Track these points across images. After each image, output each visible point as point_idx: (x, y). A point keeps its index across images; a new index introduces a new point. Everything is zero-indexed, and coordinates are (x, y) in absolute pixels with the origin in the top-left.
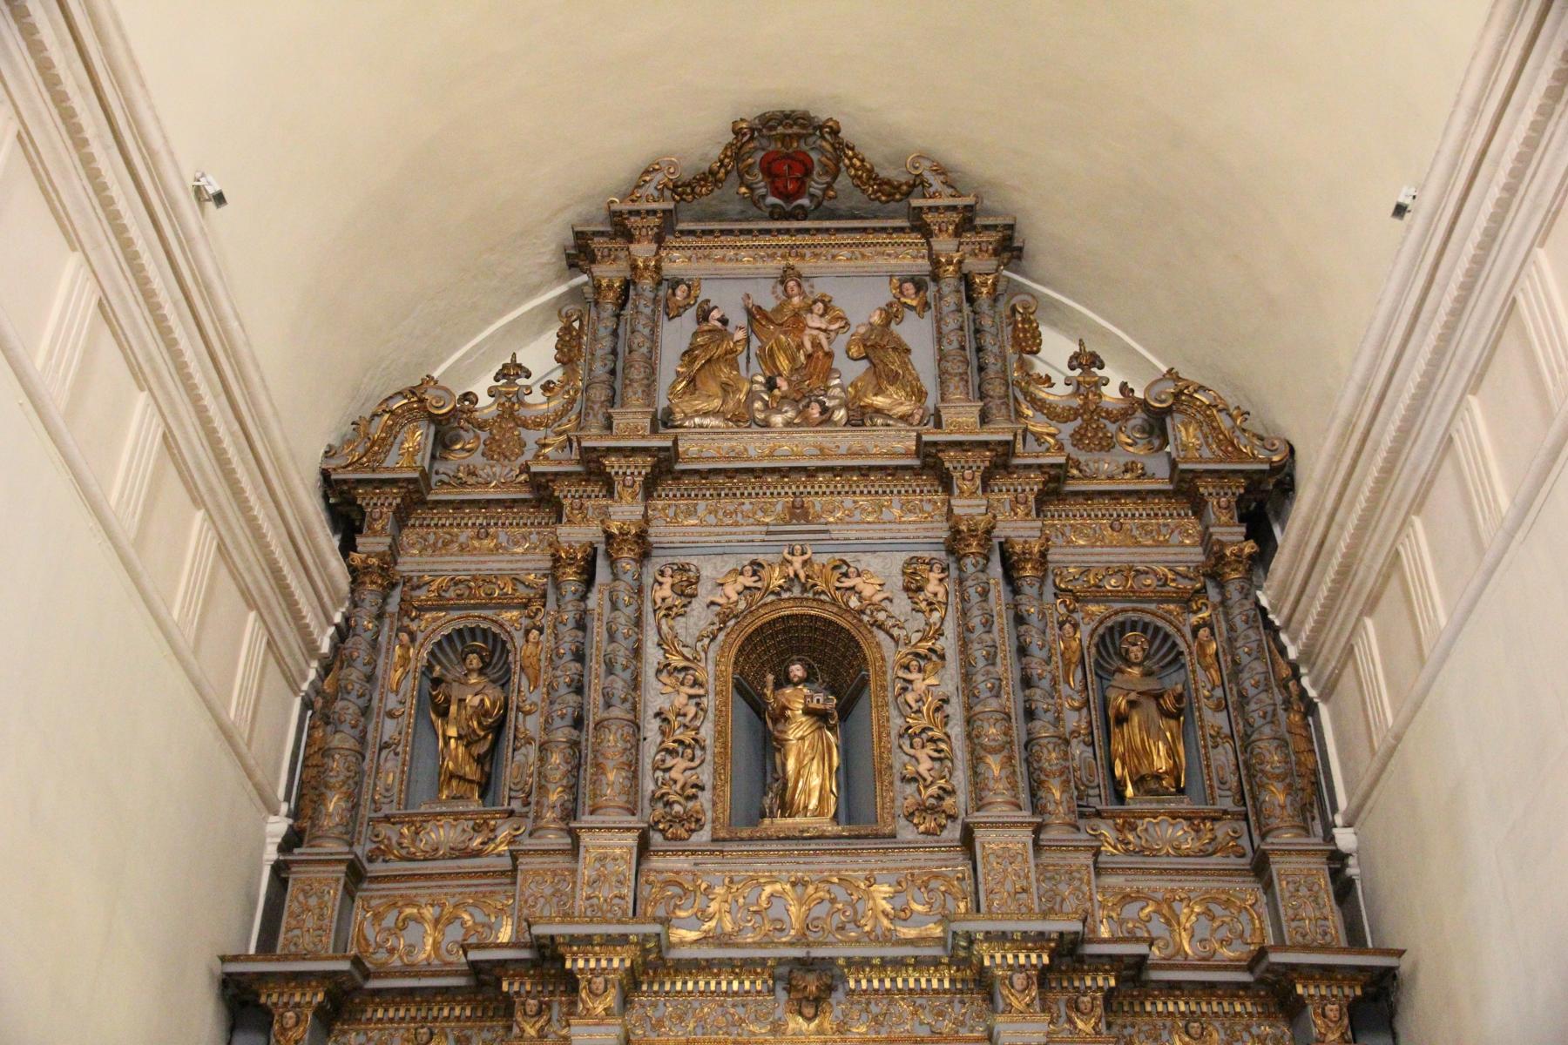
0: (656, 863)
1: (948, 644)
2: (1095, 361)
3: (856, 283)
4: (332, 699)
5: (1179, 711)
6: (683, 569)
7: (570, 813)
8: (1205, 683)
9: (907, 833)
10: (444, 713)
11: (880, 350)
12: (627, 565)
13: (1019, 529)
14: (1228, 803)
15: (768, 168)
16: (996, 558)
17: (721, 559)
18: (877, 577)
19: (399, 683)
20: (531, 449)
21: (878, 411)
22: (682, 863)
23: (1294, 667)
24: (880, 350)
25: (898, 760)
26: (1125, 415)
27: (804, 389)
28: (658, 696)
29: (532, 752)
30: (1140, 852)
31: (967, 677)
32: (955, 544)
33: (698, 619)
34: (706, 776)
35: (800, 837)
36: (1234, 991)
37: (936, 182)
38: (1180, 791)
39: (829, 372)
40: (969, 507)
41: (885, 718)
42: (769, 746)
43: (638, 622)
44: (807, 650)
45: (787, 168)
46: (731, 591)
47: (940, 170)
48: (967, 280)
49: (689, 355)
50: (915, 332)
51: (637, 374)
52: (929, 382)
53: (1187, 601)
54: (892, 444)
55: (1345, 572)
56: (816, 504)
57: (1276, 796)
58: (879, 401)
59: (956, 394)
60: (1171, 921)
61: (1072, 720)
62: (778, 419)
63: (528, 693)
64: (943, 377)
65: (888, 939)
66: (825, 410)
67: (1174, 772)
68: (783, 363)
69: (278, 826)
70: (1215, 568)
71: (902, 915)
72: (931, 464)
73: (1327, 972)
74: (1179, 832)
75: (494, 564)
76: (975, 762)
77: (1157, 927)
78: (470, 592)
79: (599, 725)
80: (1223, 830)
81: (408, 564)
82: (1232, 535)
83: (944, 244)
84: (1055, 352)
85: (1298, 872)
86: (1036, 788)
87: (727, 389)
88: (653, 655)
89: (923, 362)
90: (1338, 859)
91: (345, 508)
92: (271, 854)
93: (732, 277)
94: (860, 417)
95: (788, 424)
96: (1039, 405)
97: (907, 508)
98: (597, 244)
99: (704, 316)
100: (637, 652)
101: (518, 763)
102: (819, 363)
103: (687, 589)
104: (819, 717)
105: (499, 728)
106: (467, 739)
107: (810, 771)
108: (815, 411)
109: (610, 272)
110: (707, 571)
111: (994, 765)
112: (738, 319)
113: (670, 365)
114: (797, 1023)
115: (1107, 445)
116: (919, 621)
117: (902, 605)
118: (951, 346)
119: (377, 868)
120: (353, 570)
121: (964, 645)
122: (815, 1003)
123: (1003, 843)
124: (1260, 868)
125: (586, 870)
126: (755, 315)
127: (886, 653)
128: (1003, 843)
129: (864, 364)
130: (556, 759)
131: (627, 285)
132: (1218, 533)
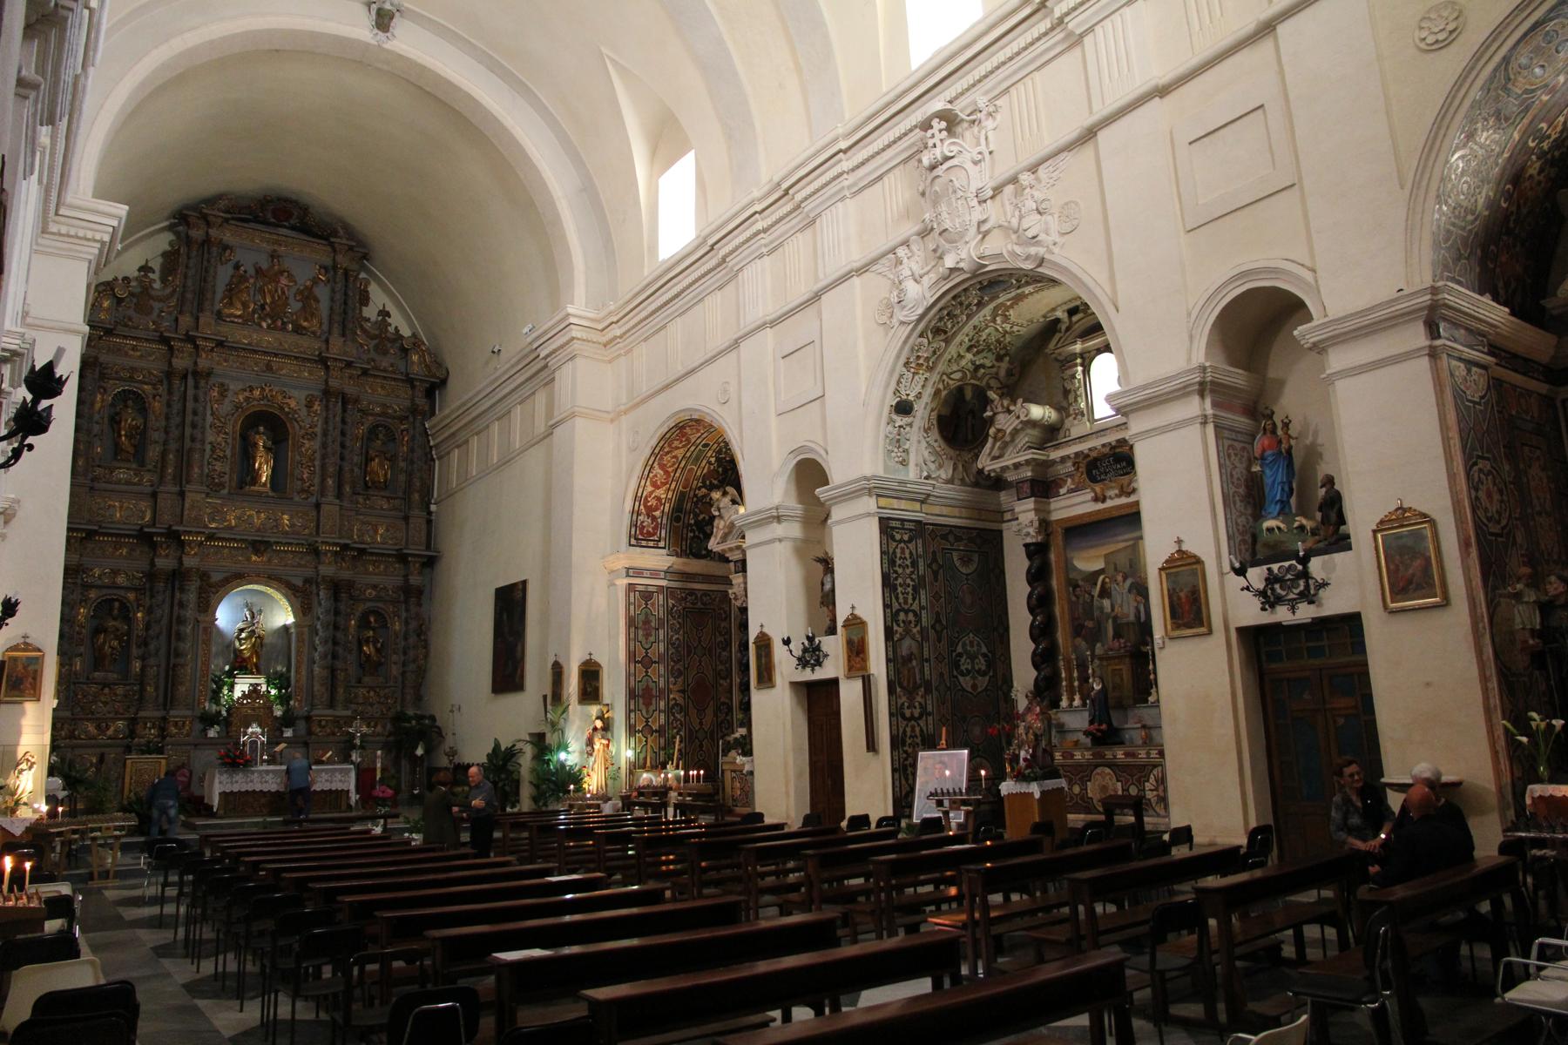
1: (318, 430)
2: (388, 314)
3: (304, 263)
5: (393, 459)
6: (222, 385)
9: (297, 499)
13: (351, 389)
14: (400, 494)
17: (235, 387)
18: (295, 401)
24: (307, 296)
25: (297, 472)
26: (393, 341)
27: (275, 315)
29: (158, 448)
31: (324, 446)
32: (327, 393)
33: (226, 407)
34: (227, 470)
35: (260, 494)
37: (341, 232)
39: (286, 304)
42: (247, 454)
45: (280, 212)
47: (347, 227)
48: (346, 273)
50: (322, 293)
53: (402, 419)
54: (309, 345)
55: (453, 434)
57: (416, 496)
60: (376, 532)
66: (284, 323)
70: (414, 410)
71: (292, 525)
72: (323, 361)
76: (323, 480)
79: (190, 450)
80: (397, 502)
81: (103, 358)
82: (421, 401)
85: (417, 520)
87: (245, 305)
88: (209, 419)
90: (430, 513)
93: (250, 248)
94: (298, 330)
96: (364, 330)
99: (237, 267)
101: (153, 452)
103: (223, 394)
109: (197, 234)
112: (251, 271)
114: (254, 558)
115: (385, 353)
117: (304, 410)
119: (97, 485)
122: (257, 552)
124: (406, 519)
126: (259, 271)
128: (330, 508)
129: (300, 305)
132: (417, 401)
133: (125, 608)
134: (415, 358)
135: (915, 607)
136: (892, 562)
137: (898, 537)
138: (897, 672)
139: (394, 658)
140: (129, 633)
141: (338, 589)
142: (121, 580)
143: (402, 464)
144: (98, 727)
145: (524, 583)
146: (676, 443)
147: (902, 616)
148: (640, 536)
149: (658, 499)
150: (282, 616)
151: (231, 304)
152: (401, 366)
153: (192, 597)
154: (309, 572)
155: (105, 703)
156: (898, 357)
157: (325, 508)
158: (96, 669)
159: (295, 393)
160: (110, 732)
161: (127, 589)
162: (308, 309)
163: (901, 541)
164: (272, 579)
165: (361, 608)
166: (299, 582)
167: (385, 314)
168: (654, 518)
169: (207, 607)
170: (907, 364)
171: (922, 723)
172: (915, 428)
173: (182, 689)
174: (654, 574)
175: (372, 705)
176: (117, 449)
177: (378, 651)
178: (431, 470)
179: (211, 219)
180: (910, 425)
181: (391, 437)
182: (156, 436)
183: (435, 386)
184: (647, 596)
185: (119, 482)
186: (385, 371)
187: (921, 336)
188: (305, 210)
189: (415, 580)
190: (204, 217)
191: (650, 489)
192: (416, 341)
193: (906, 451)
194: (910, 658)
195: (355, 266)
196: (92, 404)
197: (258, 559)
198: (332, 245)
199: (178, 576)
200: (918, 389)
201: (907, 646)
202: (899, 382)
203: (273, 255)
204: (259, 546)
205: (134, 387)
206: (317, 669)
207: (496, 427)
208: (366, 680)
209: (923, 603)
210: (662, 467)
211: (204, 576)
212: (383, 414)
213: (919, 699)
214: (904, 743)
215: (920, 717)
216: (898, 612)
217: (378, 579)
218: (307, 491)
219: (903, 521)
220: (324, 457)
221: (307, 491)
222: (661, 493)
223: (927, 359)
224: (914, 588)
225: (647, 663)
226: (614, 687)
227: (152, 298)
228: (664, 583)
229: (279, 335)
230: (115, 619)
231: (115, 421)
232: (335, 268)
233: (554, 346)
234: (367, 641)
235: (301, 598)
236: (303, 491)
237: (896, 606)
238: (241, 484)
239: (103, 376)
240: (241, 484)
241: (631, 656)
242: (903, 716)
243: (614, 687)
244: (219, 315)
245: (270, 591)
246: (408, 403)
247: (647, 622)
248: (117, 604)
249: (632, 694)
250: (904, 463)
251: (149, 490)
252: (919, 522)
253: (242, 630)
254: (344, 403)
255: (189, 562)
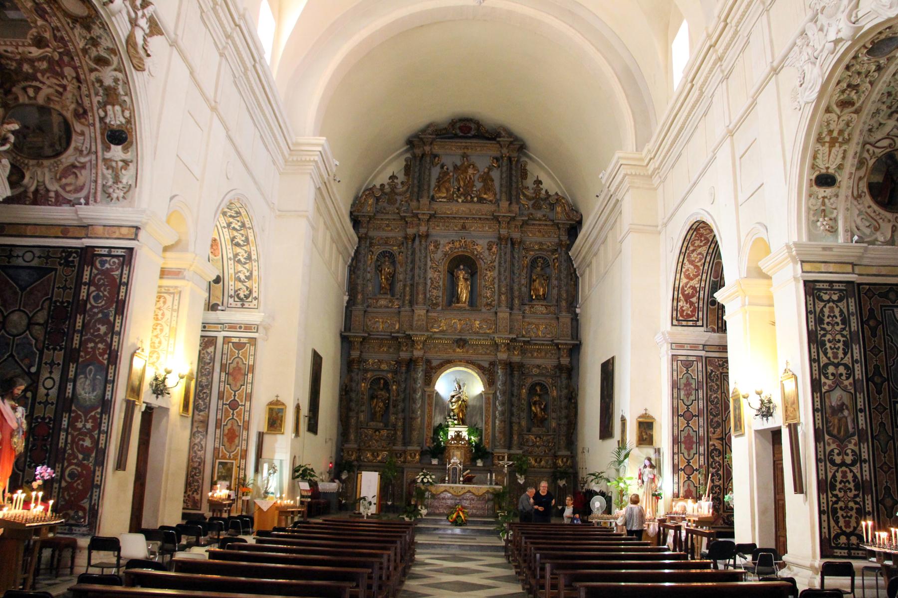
0: (430, 314)
1: (496, 264)
2: (541, 183)
3: (482, 158)
4: (354, 269)
6: (436, 241)
7: (411, 303)
8: (554, 273)
9: (484, 310)
10: (381, 271)
11: (486, 178)
12: (423, 242)
13: (516, 235)
14: (554, 303)
15: (461, 128)
16: (509, 242)
17: (445, 241)
18: (481, 247)
19: (370, 260)
20: (399, 202)
21: (485, 199)
22: (435, 314)
23: (575, 270)
24: (486, 178)
27: (466, 193)
28: (430, 274)
30: (534, 313)
31: (500, 273)
33: (439, 255)
35: (460, 309)
36: (547, 345)
37: (503, 134)
38: (545, 299)
39: (474, 186)
40: (504, 232)
41: (480, 282)
43: (426, 257)
44: (464, 262)
45: (465, 129)
46: (447, 248)
48: (510, 159)
49: (439, 180)
50: (495, 174)
51: (426, 187)
52: (498, 190)
55: (584, 258)
56: (468, 226)
57: (564, 304)
58: (485, 196)
59: (504, 198)
60: (538, 329)
61: (523, 281)
62: (460, 200)
63: (400, 269)
64: (501, 192)
65: (478, 333)
66: (472, 198)
67: (544, 295)
68: (462, 184)
69: (346, 298)
70: (560, 244)
71: (481, 327)
72: (496, 219)
73: (566, 344)
74: (543, 309)
75: (391, 234)
76: (500, 296)
77: (535, 330)
78: (386, 241)
80: (552, 309)
81: (371, 234)
82: (565, 238)
83: (505, 151)
84: (530, 182)
86: (513, 299)
87: (448, 190)
88: (429, 263)
89: (497, 184)
90: (577, 315)
91: (356, 222)
92: (345, 304)
93: (450, 155)
94: (481, 200)
95: (463, 202)
96: (525, 195)
97: (490, 228)
98: (416, 143)
99: (442, 167)
100: (426, 265)
101: (399, 286)
102: (470, 184)
103: (437, 246)
104: (466, 280)
105: (393, 277)
106: (387, 279)
107: (464, 294)
108: (469, 198)
109: (418, 152)
110: (442, 242)
111: (503, 297)
112: (451, 168)
113: (433, 183)
114: (458, 350)
115: (540, 208)
116: (489, 258)
117: (487, 252)
118: (504, 182)
119: (369, 309)
120: (359, 238)
121: (499, 266)
123: (504, 314)
125: (416, 318)
126: (456, 167)
127: (481, 265)
129: (482, 184)
130: (408, 289)
131: (423, 155)
133: (386, 384)
134: (559, 209)
135: (847, 360)
136: (819, 321)
137: (826, 297)
138: (826, 421)
139: (554, 415)
140: (389, 399)
141: (510, 367)
142: (384, 367)
143: (555, 282)
144: (373, 455)
145: (613, 358)
146: (697, 243)
147: (831, 369)
148: (680, 318)
149: (694, 288)
150: (476, 387)
151: (439, 190)
152: (551, 215)
153: (420, 374)
154: (491, 358)
155: (377, 441)
156: (808, 134)
157: (500, 315)
158: (373, 420)
159: (480, 242)
160: (379, 458)
161: (388, 371)
162: (487, 188)
163: (829, 301)
164: (469, 363)
165: (529, 381)
166: (486, 365)
167: (538, 182)
168: (692, 304)
169: (429, 380)
170: (819, 140)
171: (854, 469)
172: (842, 197)
173: (415, 433)
174: (694, 347)
175: (538, 447)
176: (381, 288)
177: (541, 409)
178: (576, 285)
179: (425, 140)
180: (837, 196)
181: (546, 264)
182: (401, 277)
183: (574, 228)
184: (688, 364)
185: (381, 307)
186: (540, 220)
187: (828, 110)
188: (478, 123)
189: (565, 361)
190: (421, 139)
191: (684, 280)
192: (559, 199)
193: (835, 220)
194: (841, 407)
195: (515, 154)
196: (365, 262)
197: (461, 350)
198: (499, 142)
199: (411, 363)
200: (839, 161)
201: (836, 397)
202: (815, 158)
203: (465, 156)
204: (461, 343)
205: (387, 248)
206: (497, 422)
207: (602, 248)
208: (534, 429)
209: (856, 356)
210: (691, 262)
211: (428, 362)
212: (540, 249)
213: (851, 446)
214: (833, 487)
215: (853, 463)
216: (826, 366)
217: (542, 362)
218: (490, 305)
219: (831, 283)
220: (500, 279)
221: (490, 305)
222: (695, 283)
223: (841, 132)
224: (845, 343)
225: (688, 416)
226: (663, 436)
227: (396, 194)
228: (703, 353)
229: (468, 205)
230: (382, 390)
231: (379, 269)
232: (502, 157)
233: (617, 183)
234: (535, 403)
235: (488, 373)
236: (487, 304)
237: (824, 360)
238: (450, 303)
239: (371, 244)
240: (450, 303)
241: (675, 411)
242: (833, 462)
243: (663, 436)
244: (433, 198)
245: (470, 371)
246: (557, 240)
247: (688, 384)
248: (382, 381)
249: (676, 441)
250: (833, 230)
251: (396, 311)
252: (852, 282)
253: (453, 397)
254: (513, 244)
255: (417, 353)
